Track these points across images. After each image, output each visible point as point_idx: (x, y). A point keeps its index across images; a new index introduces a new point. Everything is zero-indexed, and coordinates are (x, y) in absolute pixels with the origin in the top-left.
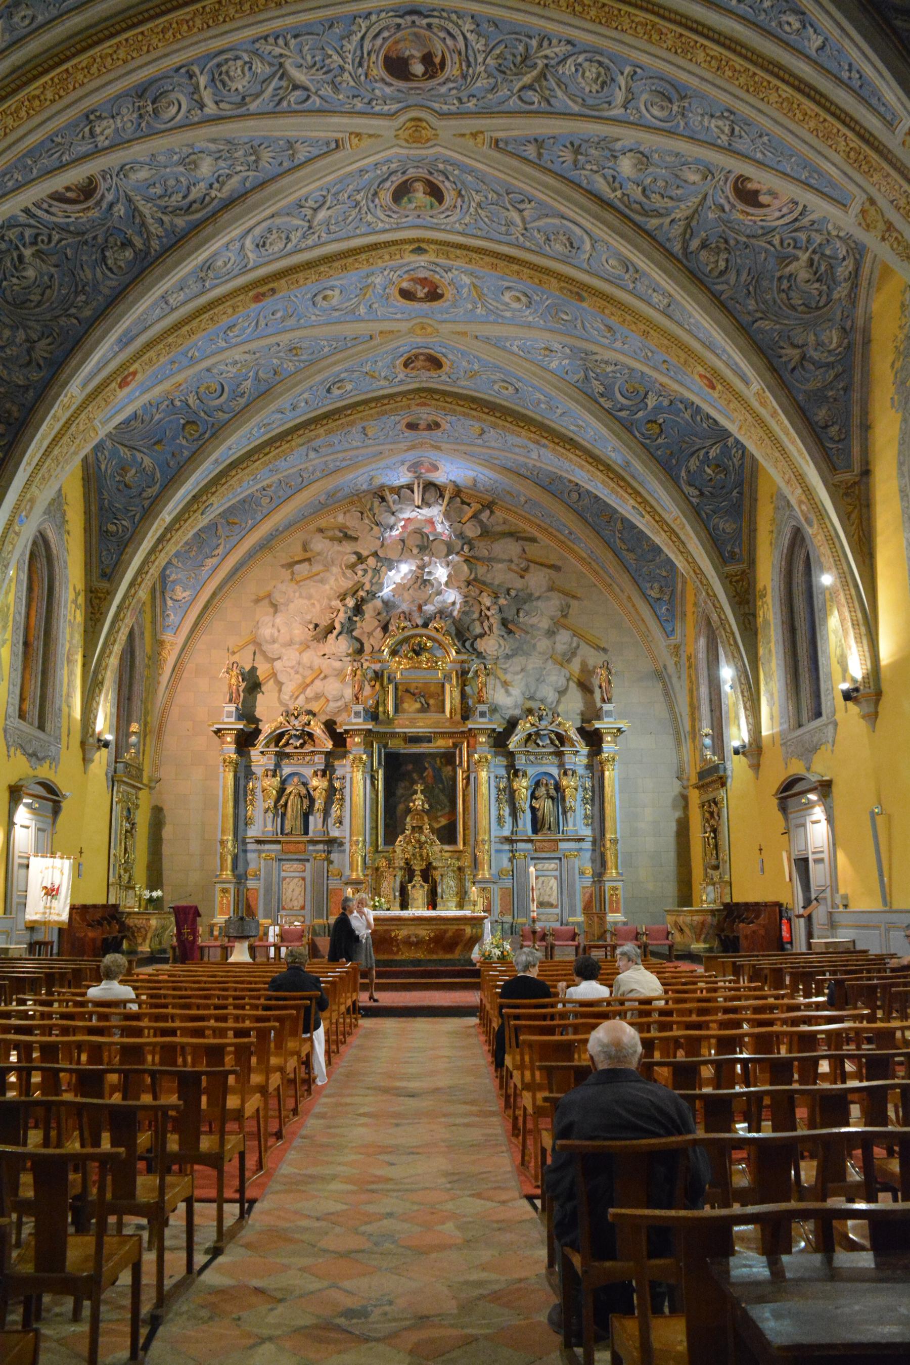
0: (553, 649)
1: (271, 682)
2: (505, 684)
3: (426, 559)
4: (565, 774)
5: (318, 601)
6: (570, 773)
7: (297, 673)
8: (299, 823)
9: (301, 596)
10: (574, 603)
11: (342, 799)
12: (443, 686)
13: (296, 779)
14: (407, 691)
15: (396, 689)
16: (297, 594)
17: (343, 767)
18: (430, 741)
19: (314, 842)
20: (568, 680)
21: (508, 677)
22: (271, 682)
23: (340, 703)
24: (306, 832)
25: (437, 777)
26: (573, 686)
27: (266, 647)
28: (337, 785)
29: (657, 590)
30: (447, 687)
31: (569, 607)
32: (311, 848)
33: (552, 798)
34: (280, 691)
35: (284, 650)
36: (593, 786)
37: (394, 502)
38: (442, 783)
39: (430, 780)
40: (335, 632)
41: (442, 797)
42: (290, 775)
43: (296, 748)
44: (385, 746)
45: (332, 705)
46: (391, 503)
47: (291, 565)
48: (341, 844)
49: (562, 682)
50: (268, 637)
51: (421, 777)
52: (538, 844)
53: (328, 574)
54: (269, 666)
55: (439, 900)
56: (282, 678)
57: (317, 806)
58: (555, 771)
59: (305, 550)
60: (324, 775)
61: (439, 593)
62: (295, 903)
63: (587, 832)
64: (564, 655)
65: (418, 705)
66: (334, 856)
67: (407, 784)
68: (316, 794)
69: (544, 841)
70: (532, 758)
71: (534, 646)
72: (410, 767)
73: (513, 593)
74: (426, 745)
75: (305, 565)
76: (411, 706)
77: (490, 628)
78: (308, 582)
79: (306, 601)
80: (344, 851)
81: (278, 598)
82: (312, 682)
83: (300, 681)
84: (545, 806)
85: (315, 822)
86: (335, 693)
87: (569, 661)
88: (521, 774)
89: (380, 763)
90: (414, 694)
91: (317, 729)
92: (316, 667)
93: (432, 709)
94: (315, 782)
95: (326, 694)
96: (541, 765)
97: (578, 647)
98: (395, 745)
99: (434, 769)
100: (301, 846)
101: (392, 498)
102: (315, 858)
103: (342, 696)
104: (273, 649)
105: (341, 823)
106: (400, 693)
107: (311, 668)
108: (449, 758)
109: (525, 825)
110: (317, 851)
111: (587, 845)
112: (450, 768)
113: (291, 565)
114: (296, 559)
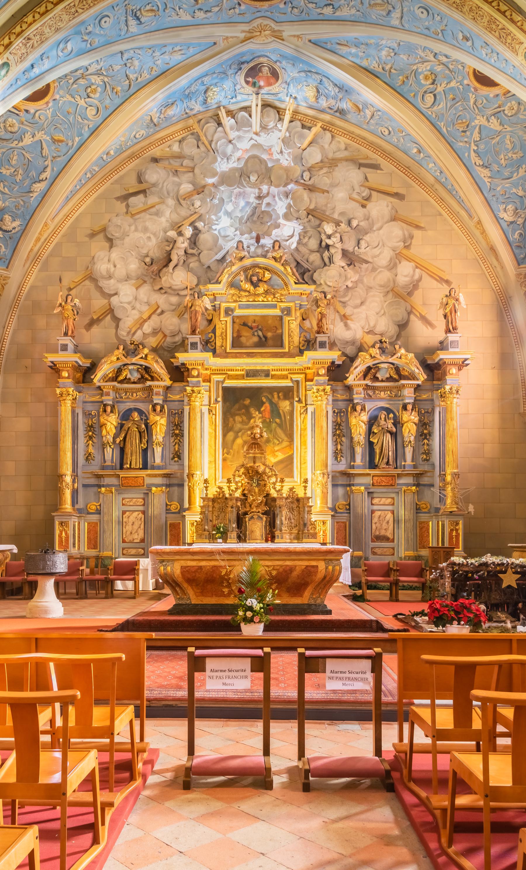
0: (394, 281)
1: (109, 317)
2: (344, 318)
3: (265, 188)
5: (154, 234)
7: (134, 308)
9: (136, 230)
10: (417, 233)
16: (133, 228)
21: (348, 311)
22: (109, 317)
27: (102, 283)
29: (510, 212)
31: (411, 237)
34: (117, 327)
35: (120, 286)
37: (232, 128)
39: (267, 415)
40: (172, 265)
46: (228, 129)
47: (125, 198)
50: (104, 273)
53: (162, 207)
54: (106, 301)
55: (277, 533)
56: (118, 314)
59: (140, 182)
61: (278, 226)
62: (136, 536)
65: (256, 339)
70: (370, 392)
73: (354, 223)
75: (141, 197)
77: (330, 259)
78: (143, 214)
79: (141, 235)
81: (113, 231)
82: (149, 318)
83: (136, 317)
86: (171, 328)
90: (251, 328)
92: (153, 302)
93: (270, 342)
95: (164, 329)
99: (271, 403)
101: (228, 122)
104: (109, 285)
105: (179, 457)
107: (148, 303)
113: (125, 198)
114: (131, 191)
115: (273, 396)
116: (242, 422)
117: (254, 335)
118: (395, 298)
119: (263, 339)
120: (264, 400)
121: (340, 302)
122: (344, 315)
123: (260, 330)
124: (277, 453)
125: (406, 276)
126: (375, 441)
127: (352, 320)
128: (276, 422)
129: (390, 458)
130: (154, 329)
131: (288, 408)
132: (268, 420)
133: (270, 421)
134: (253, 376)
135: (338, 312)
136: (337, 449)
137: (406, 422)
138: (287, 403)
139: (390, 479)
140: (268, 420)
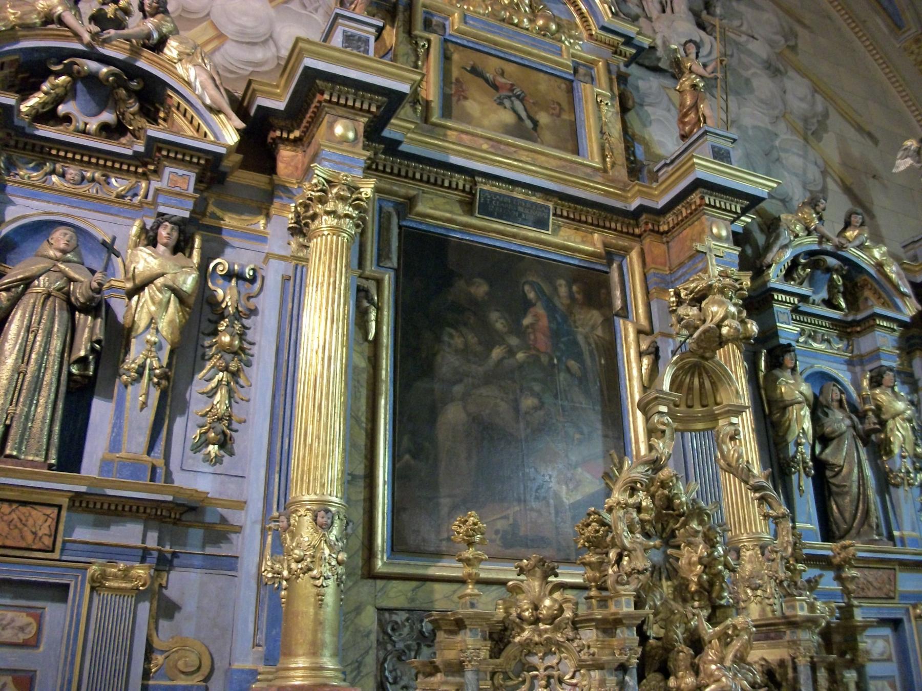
0: (784, 103)
4: (876, 381)
8: (44, 409)
11: (241, 352)
12: (571, 90)
13: (60, 238)
14: (475, 71)
15: (446, 58)
17: (256, 242)
18: (541, 224)
19: (99, 507)
20: (824, 173)
23: (259, 54)
24: (70, 455)
26: (832, 186)
28: (226, 295)
30: (585, 91)
32: (83, 534)
38: (579, 357)
42: (40, 229)
43: (84, 132)
44: (406, 205)
45: (233, 54)
48: (220, 532)
49: (813, 173)
57: (136, 355)
58: (844, 376)
60: (181, 247)
66: (183, 583)
67: (472, 339)
68: (143, 309)
76: (486, 115)
80: (230, 564)
85: (116, 426)
87: (817, 135)
88: (788, 359)
89: (382, 255)
90: (495, 87)
91: (187, 72)
93: (547, 135)
94: (145, 261)
95: (216, 16)
97: (826, 115)
98: (437, 210)
99: (551, 309)
100: (39, 521)
102: (97, 585)
103: (269, 39)
105: (225, 443)
106: (455, 73)
108: (593, 285)
110: (113, 552)
112: (596, 316)
115: (555, 289)
116: (465, 352)
119: (529, 124)
120: (532, 295)
123: (522, 99)
126: (831, 460)
128: (568, 370)
130: (184, 10)
131: (599, 332)
140: (544, 359)
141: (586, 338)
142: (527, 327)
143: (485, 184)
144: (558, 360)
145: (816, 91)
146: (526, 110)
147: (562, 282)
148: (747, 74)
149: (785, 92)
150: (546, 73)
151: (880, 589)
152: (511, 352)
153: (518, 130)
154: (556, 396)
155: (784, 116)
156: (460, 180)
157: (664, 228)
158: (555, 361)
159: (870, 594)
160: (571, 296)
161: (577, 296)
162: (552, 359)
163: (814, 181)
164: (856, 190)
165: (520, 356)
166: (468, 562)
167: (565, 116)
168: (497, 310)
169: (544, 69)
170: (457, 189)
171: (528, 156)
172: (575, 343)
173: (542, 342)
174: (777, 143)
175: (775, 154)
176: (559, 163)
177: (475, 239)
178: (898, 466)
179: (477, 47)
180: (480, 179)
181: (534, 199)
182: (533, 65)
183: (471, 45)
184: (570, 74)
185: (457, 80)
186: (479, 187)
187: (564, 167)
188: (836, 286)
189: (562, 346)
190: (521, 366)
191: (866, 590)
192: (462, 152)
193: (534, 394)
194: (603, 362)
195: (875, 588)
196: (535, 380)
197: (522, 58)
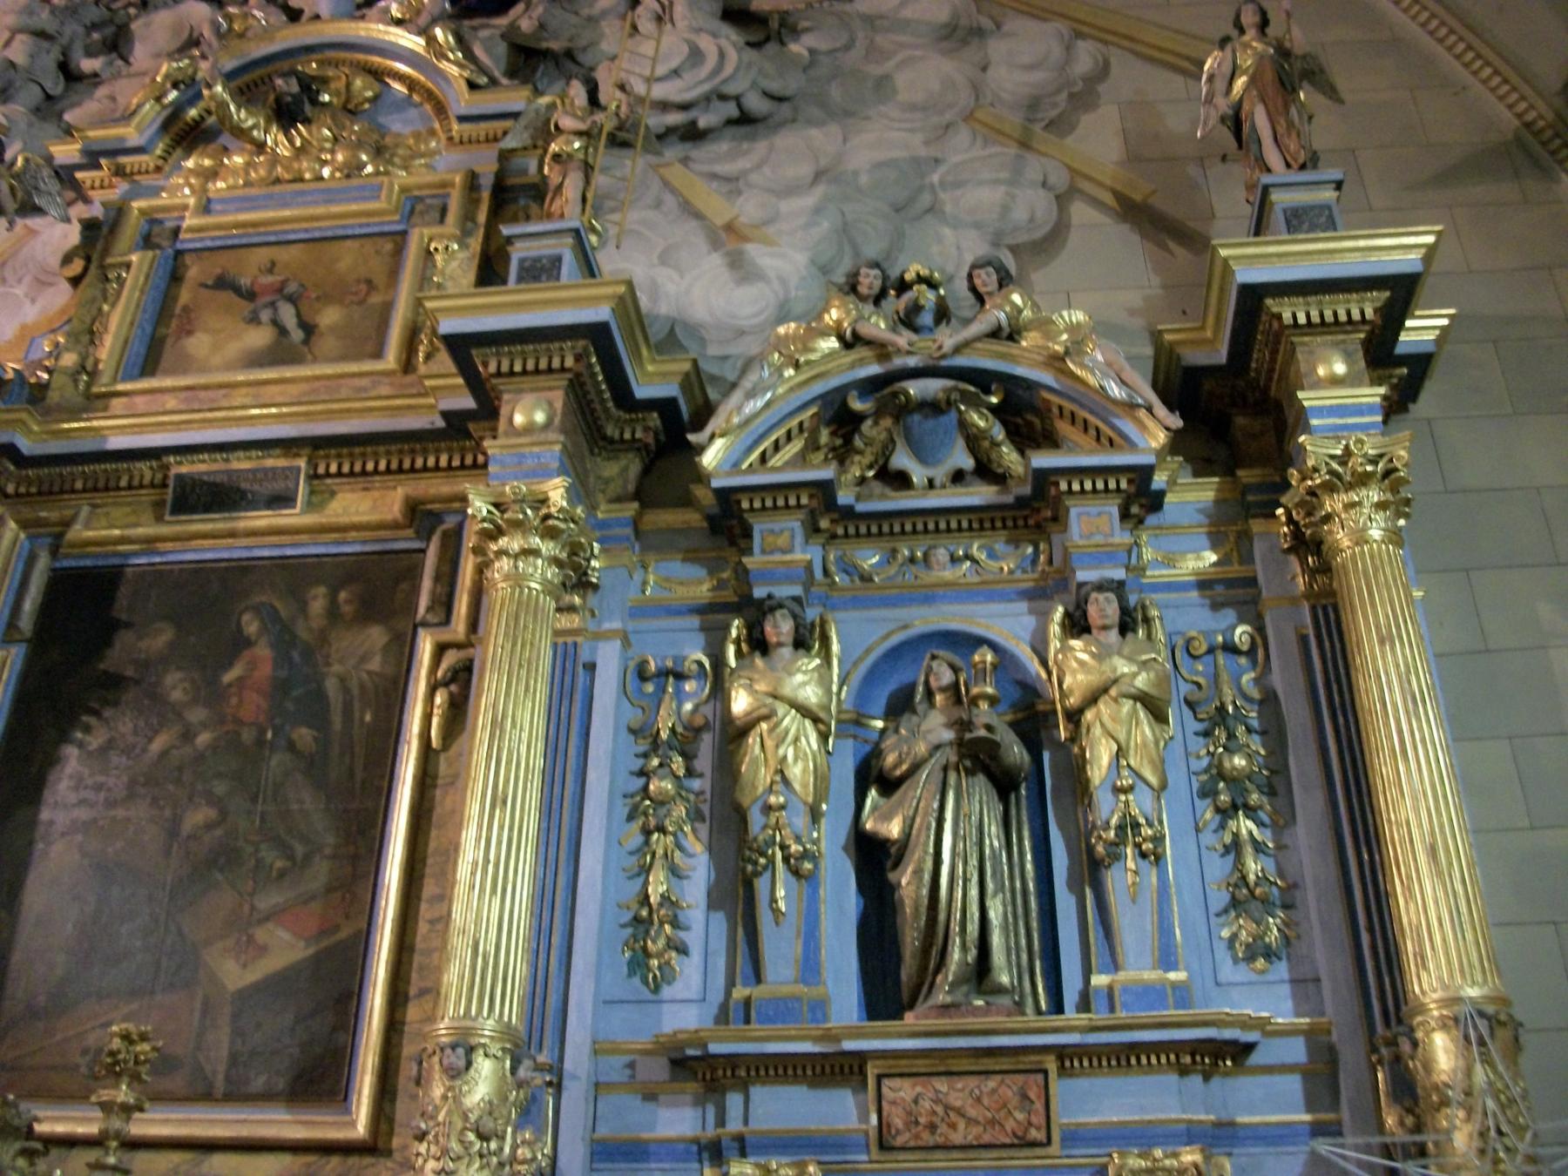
6: (1103, 609)
18: (282, 500)
21: (748, 209)
25: (298, 691)
33: (1004, 784)
36: (1269, 701)
41: (307, 802)
51: (211, 693)
52: (901, 1091)
63: (1263, 1001)
64: (1033, 105)
65: (260, 337)
69: (939, 1065)
71: (883, 86)
72: (160, 639)
74: (261, 519)
76: (220, 344)
84: (956, 843)
87: (1060, 126)
90: (250, 295)
96: (929, 595)
99: (284, 639)
109: (810, 967)
111: (1270, 1099)
117: (254, 320)
118: (986, 142)
119: (297, 335)
120: (251, 626)
121: (714, 176)
122: (730, 228)
123: (292, 300)
124: (261, 934)
125: (1030, 67)
127: (767, 242)
128: (291, 747)
129: (996, 940)
132: (247, 736)
133: (260, 742)
134: (207, 510)
135: (698, 216)
136: (645, 899)
137: (1093, 699)
138: (377, 636)
139: (1008, 1089)
140: (247, 736)
141: (342, 680)
142: (230, 685)
143: (180, 463)
144: (274, 735)
145: (1079, 35)
146: (298, 315)
147: (322, 590)
148: (876, 70)
149: (984, 69)
150: (294, 242)
151: (993, 1122)
152: (188, 736)
153: (280, 353)
154: (254, 799)
155: (969, 117)
156: (144, 468)
157: (611, 430)
158: (269, 735)
159: (957, 1138)
160: (333, 612)
161: (347, 609)
162: (262, 732)
163: (1032, 220)
164: (1160, 203)
165: (204, 738)
166: (107, 1107)
167: (376, 299)
168: (179, 668)
169: (350, 232)
170: (141, 486)
171: (247, 395)
172: (320, 695)
173: (252, 705)
174: (935, 178)
175: (926, 199)
176: (304, 387)
177: (171, 558)
178: (1104, 814)
179: (230, 242)
180: (172, 459)
181: (269, 463)
182: (329, 234)
183: (218, 243)
184: (398, 222)
185: (186, 309)
186: (174, 471)
187: (314, 391)
188: (983, 434)
189: (290, 706)
190: (200, 758)
191: (943, 1128)
192: (125, 426)
193: (212, 800)
194: (368, 718)
195: (971, 1121)
196: (219, 775)
197: (306, 230)
